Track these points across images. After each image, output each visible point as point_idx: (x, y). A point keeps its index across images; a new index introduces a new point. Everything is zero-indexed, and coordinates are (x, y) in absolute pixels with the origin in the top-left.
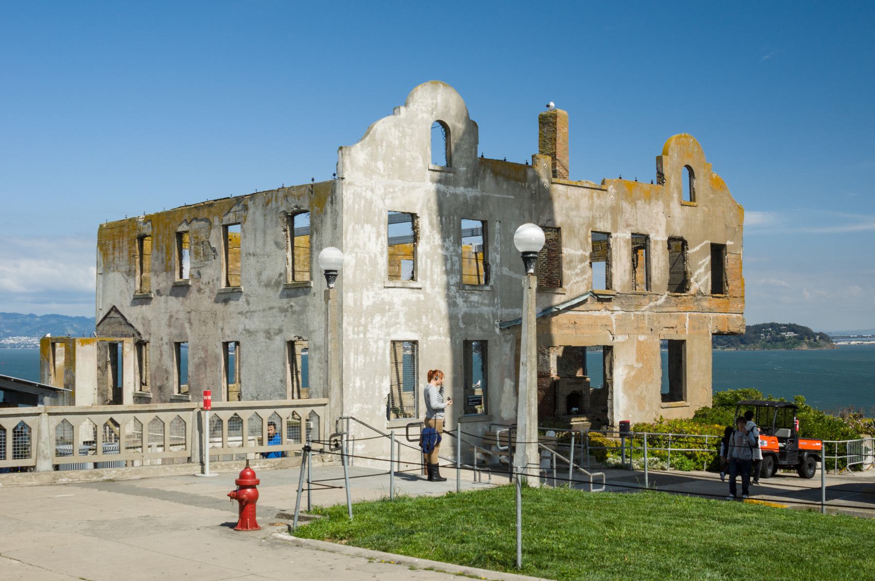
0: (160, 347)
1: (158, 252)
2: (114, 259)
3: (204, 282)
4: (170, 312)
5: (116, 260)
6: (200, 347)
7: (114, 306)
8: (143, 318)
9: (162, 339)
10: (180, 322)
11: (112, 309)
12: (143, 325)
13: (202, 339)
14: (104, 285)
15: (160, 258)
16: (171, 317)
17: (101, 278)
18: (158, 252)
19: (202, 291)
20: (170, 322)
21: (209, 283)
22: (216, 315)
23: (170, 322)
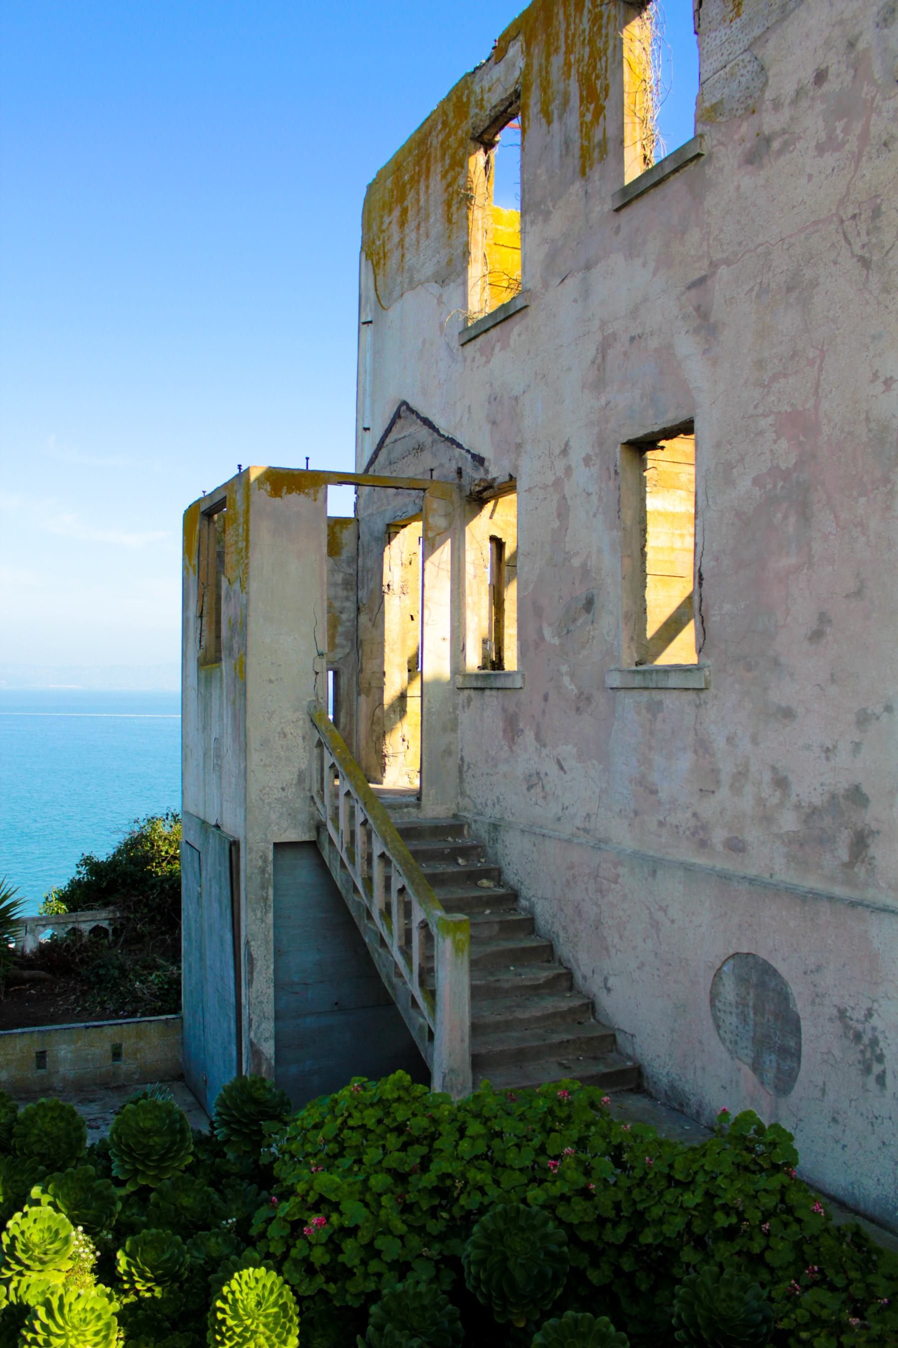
0: (558, 483)
1: (549, 123)
2: (403, 256)
3: (789, 89)
4: (603, 324)
5: (408, 256)
6: (764, 423)
7: (404, 403)
8: (494, 399)
9: (565, 452)
10: (653, 343)
11: (397, 416)
12: (494, 423)
13: (774, 378)
14: (378, 353)
15: (558, 140)
16: (604, 348)
17: (368, 330)
18: (549, 123)
19: (776, 145)
20: (601, 368)
21: (820, 77)
22: (876, 213)
23: (601, 368)
